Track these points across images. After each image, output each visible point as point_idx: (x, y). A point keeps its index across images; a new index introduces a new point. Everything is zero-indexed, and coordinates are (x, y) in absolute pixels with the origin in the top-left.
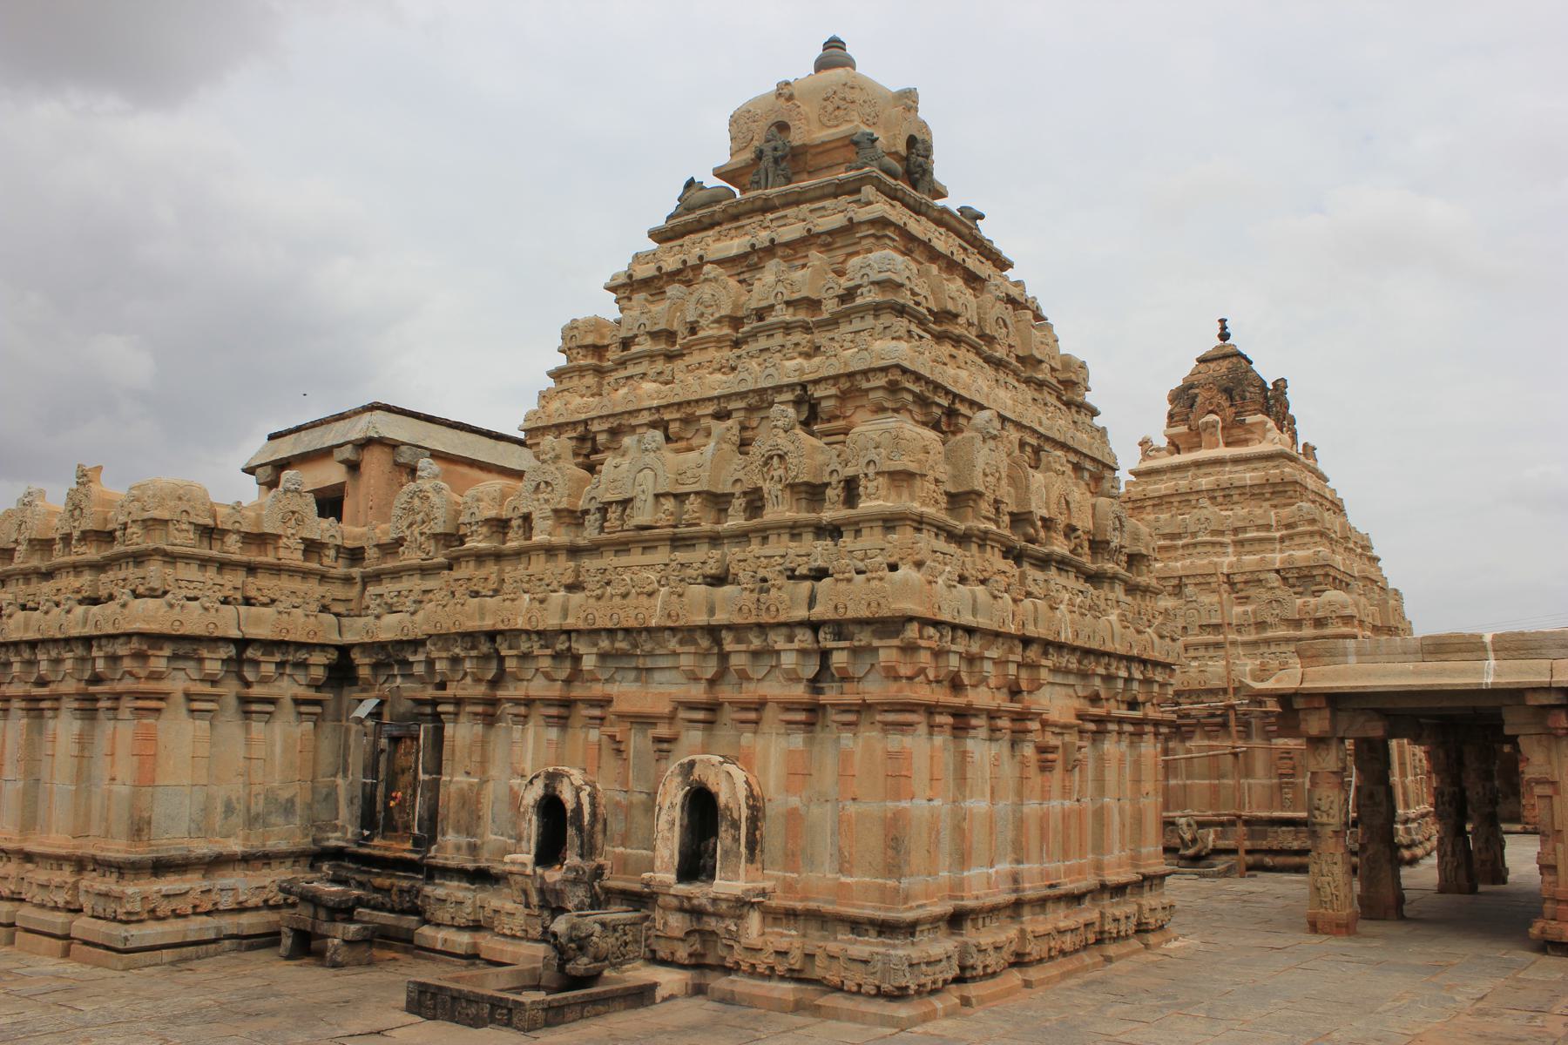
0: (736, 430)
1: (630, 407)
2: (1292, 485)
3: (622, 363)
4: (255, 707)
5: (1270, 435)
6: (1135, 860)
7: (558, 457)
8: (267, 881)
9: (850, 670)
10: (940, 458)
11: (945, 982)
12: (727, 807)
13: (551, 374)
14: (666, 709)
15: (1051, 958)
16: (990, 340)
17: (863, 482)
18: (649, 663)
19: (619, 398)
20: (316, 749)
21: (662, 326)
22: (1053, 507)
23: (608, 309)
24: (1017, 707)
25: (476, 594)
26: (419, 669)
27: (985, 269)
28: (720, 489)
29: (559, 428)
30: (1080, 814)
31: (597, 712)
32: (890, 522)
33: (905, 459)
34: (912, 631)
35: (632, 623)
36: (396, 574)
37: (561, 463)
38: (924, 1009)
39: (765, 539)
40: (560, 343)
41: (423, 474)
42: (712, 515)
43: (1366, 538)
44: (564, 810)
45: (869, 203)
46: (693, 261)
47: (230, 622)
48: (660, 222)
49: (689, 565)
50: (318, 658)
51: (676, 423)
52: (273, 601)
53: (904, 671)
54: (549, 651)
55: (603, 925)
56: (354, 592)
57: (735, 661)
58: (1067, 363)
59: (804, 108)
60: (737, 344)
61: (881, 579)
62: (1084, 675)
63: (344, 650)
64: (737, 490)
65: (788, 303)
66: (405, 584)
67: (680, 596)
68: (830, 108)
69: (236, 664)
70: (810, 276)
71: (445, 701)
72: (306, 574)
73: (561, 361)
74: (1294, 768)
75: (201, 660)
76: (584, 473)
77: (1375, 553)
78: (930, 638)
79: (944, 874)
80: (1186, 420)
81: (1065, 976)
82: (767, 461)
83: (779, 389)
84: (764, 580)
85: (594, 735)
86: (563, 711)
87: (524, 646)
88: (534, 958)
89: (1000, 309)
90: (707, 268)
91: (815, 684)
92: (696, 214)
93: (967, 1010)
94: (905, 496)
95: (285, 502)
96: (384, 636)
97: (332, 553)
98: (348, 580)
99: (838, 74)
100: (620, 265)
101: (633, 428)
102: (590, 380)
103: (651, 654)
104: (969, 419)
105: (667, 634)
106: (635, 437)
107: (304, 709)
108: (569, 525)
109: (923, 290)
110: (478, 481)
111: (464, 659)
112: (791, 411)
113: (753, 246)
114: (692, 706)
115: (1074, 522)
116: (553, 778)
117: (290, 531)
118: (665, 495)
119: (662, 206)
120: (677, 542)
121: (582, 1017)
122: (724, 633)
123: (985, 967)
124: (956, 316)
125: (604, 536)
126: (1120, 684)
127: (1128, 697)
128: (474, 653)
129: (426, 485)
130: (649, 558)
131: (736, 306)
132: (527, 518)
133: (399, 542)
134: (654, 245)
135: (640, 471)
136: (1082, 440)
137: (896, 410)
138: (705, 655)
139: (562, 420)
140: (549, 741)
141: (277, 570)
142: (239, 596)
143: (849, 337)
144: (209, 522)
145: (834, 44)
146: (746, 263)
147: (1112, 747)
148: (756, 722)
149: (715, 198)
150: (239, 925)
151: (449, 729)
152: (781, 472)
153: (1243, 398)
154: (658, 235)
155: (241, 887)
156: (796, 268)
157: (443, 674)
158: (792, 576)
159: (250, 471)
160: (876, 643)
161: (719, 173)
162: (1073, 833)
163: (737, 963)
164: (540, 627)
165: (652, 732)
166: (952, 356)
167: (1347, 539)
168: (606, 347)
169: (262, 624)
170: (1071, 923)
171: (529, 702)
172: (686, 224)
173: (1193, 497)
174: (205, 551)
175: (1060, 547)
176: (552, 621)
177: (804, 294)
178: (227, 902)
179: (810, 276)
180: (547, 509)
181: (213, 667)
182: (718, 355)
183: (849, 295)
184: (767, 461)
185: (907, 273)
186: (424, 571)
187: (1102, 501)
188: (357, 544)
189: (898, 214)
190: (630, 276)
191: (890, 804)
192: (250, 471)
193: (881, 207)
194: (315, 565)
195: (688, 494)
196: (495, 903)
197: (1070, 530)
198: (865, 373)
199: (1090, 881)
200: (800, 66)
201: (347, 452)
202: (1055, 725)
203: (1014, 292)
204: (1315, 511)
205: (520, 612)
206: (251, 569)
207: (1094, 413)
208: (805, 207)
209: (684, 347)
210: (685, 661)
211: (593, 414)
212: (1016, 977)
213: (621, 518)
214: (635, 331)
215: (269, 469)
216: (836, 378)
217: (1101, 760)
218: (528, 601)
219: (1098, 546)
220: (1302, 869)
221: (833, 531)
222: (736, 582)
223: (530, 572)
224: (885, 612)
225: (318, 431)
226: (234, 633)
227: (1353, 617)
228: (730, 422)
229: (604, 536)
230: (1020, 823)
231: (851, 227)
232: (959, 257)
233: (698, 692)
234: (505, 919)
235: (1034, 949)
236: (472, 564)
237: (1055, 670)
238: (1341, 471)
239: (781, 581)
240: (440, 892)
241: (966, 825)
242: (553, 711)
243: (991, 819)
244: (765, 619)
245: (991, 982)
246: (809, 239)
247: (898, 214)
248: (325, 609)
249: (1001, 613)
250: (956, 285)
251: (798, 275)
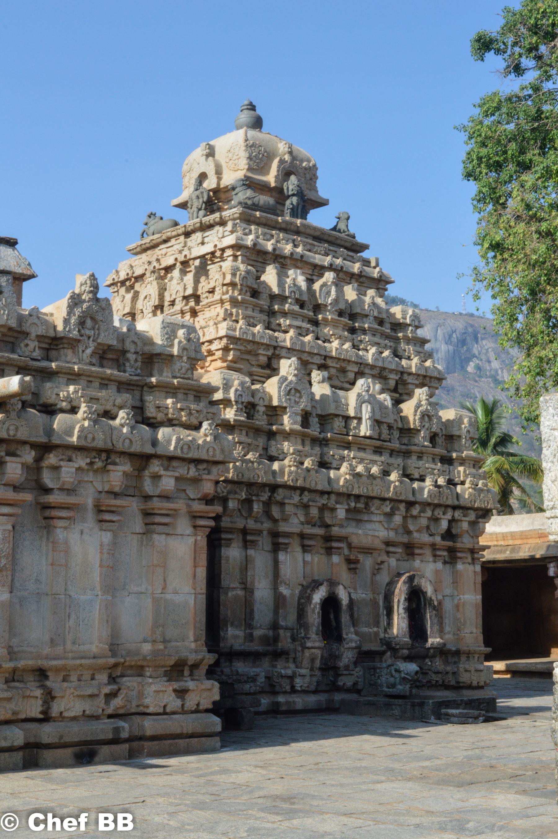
12: (431, 598)
39: (420, 458)
44: (341, 605)
103: (372, 513)
105: (388, 502)
116: (333, 584)
122: (417, 506)
244: (442, 502)
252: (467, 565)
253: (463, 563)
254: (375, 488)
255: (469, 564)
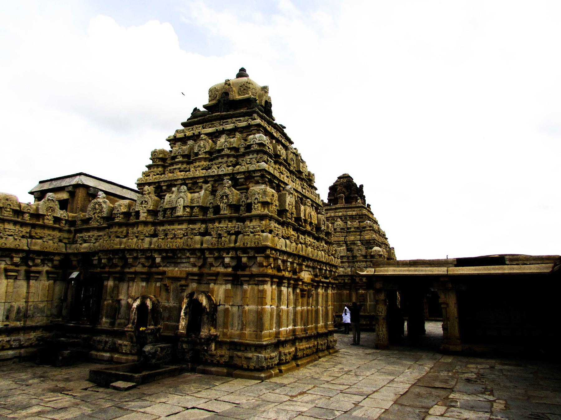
0: (210, 187)
1: (175, 178)
2: (365, 215)
3: (172, 164)
4: (32, 275)
5: (359, 201)
6: (326, 326)
7: (149, 193)
8: (32, 337)
9: (248, 263)
10: (277, 198)
11: (275, 365)
13: (147, 167)
14: (185, 276)
15: (304, 357)
16: (289, 165)
17: (253, 205)
18: (179, 261)
19: (169, 176)
20: (54, 290)
21: (186, 153)
22: (307, 216)
23: (167, 147)
24: (296, 277)
25: (118, 237)
26: (95, 262)
27: (287, 144)
28: (204, 205)
29: (149, 184)
30: (312, 310)
31: (160, 277)
32: (262, 217)
33: (267, 198)
34: (268, 252)
35: (174, 247)
36: (88, 230)
37: (151, 195)
38: (269, 374)
39: (220, 223)
40: (150, 156)
41: (100, 197)
42: (202, 214)
43: (384, 232)
44: (148, 309)
45: (255, 119)
46: (196, 132)
47: (24, 244)
48: (185, 120)
49: (194, 229)
50: (57, 258)
51: (193, 185)
52: (41, 238)
53: (265, 264)
54: (144, 256)
55: (161, 348)
56: (71, 236)
57: (210, 260)
58: (309, 173)
59: (234, 89)
60: (211, 160)
61: (259, 235)
62: (314, 268)
63: (67, 255)
64: (211, 206)
65: (229, 149)
66: (91, 234)
67: (191, 239)
68: (242, 89)
69: (25, 261)
70: (236, 141)
71: (105, 273)
72: (54, 229)
73: (151, 162)
74: (364, 299)
75: (12, 258)
76: (156, 198)
77: (386, 237)
78: (273, 254)
79: (274, 329)
80: (334, 195)
81: (308, 363)
82: (222, 197)
83: (225, 175)
84: (220, 234)
85: (158, 284)
86: (148, 277)
87: (135, 255)
88: (134, 361)
89: (291, 156)
90: (202, 136)
91: (235, 268)
92: (197, 119)
93: (280, 374)
94: (266, 210)
95: (47, 203)
96: (82, 251)
97: (64, 222)
98: (69, 231)
99: (244, 79)
100: (172, 133)
101: (175, 186)
102: (160, 169)
103: (181, 258)
104: (284, 188)
106: (177, 188)
107: (50, 275)
108: (152, 215)
109: (271, 147)
110: (117, 201)
111: (113, 259)
112: (230, 182)
113: (217, 130)
114: (193, 274)
115: (312, 221)
116: (144, 298)
117: (49, 214)
118: (187, 206)
119: (186, 116)
120: (191, 222)
121: (154, 380)
123: (286, 360)
124: (281, 156)
125: (165, 219)
126: (324, 271)
127: (325, 275)
128: (116, 257)
129: (101, 200)
130: (180, 227)
131: (211, 148)
132: (138, 213)
133: (90, 219)
134: (183, 128)
135: (180, 199)
136: (312, 197)
137: (263, 183)
138: (199, 258)
139: (151, 181)
140: (142, 286)
141: (44, 227)
142: (28, 235)
143: (249, 160)
144: (18, 208)
145: (242, 70)
146: (214, 136)
147: (320, 291)
148: (216, 280)
149: (203, 114)
150: (20, 353)
151: (105, 283)
152: (226, 201)
153: (351, 189)
154: (183, 124)
155: (22, 338)
156: (231, 138)
157: (104, 264)
158: (229, 233)
159: (31, 193)
160: (256, 255)
161: (205, 107)
162: (310, 317)
163: (206, 360)
164: (142, 248)
165: (179, 284)
166: (279, 168)
167: (380, 232)
168: (166, 159)
169: (37, 245)
170: (307, 346)
171: (136, 273)
172: (194, 122)
173: (335, 218)
174: (16, 219)
175: (308, 228)
176: (146, 246)
177: (234, 145)
178: (15, 344)
179: (236, 141)
180: (145, 210)
181: (17, 260)
182: (205, 163)
183: (249, 146)
184: (222, 197)
185: (267, 142)
186: (99, 229)
187: (319, 215)
188: (74, 219)
189: (263, 123)
190: (175, 137)
191: (260, 307)
192: (31, 193)
193: (258, 121)
194: (57, 226)
195: (194, 207)
196: (120, 342)
197: (311, 223)
198: (255, 171)
199: (314, 332)
200: (232, 76)
201: (70, 189)
202: (306, 283)
203: (295, 151)
204: (372, 223)
205: (133, 243)
206: (34, 226)
207: (316, 189)
208: (234, 119)
209: (193, 160)
210: (192, 260)
211: (161, 180)
212: (294, 364)
213: (171, 214)
214: (177, 154)
215: (39, 193)
216: (244, 173)
217: (317, 294)
218: (139, 240)
219: (318, 228)
220: (373, 330)
221: (242, 220)
222: (210, 235)
223: (139, 230)
224: (260, 245)
225: (59, 182)
226: (26, 248)
227: (382, 255)
228: (209, 185)
229: (165, 219)
230: (295, 313)
231: (249, 126)
232: (280, 139)
233: (195, 270)
234: (124, 347)
235: (300, 354)
236: (117, 227)
237: (306, 266)
238: (377, 212)
239: (226, 235)
240: (98, 338)
241: (281, 314)
242: (144, 276)
243: (288, 312)
244: (220, 246)
245: (287, 365)
246: (235, 130)
247: (263, 123)
248: (60, 241)
249: (291, 247)
250: (279, 147)
251: (232, 140)
252: (254, 286)
253: (249, 284)
254: (174, 244)
255: (256, 285)
